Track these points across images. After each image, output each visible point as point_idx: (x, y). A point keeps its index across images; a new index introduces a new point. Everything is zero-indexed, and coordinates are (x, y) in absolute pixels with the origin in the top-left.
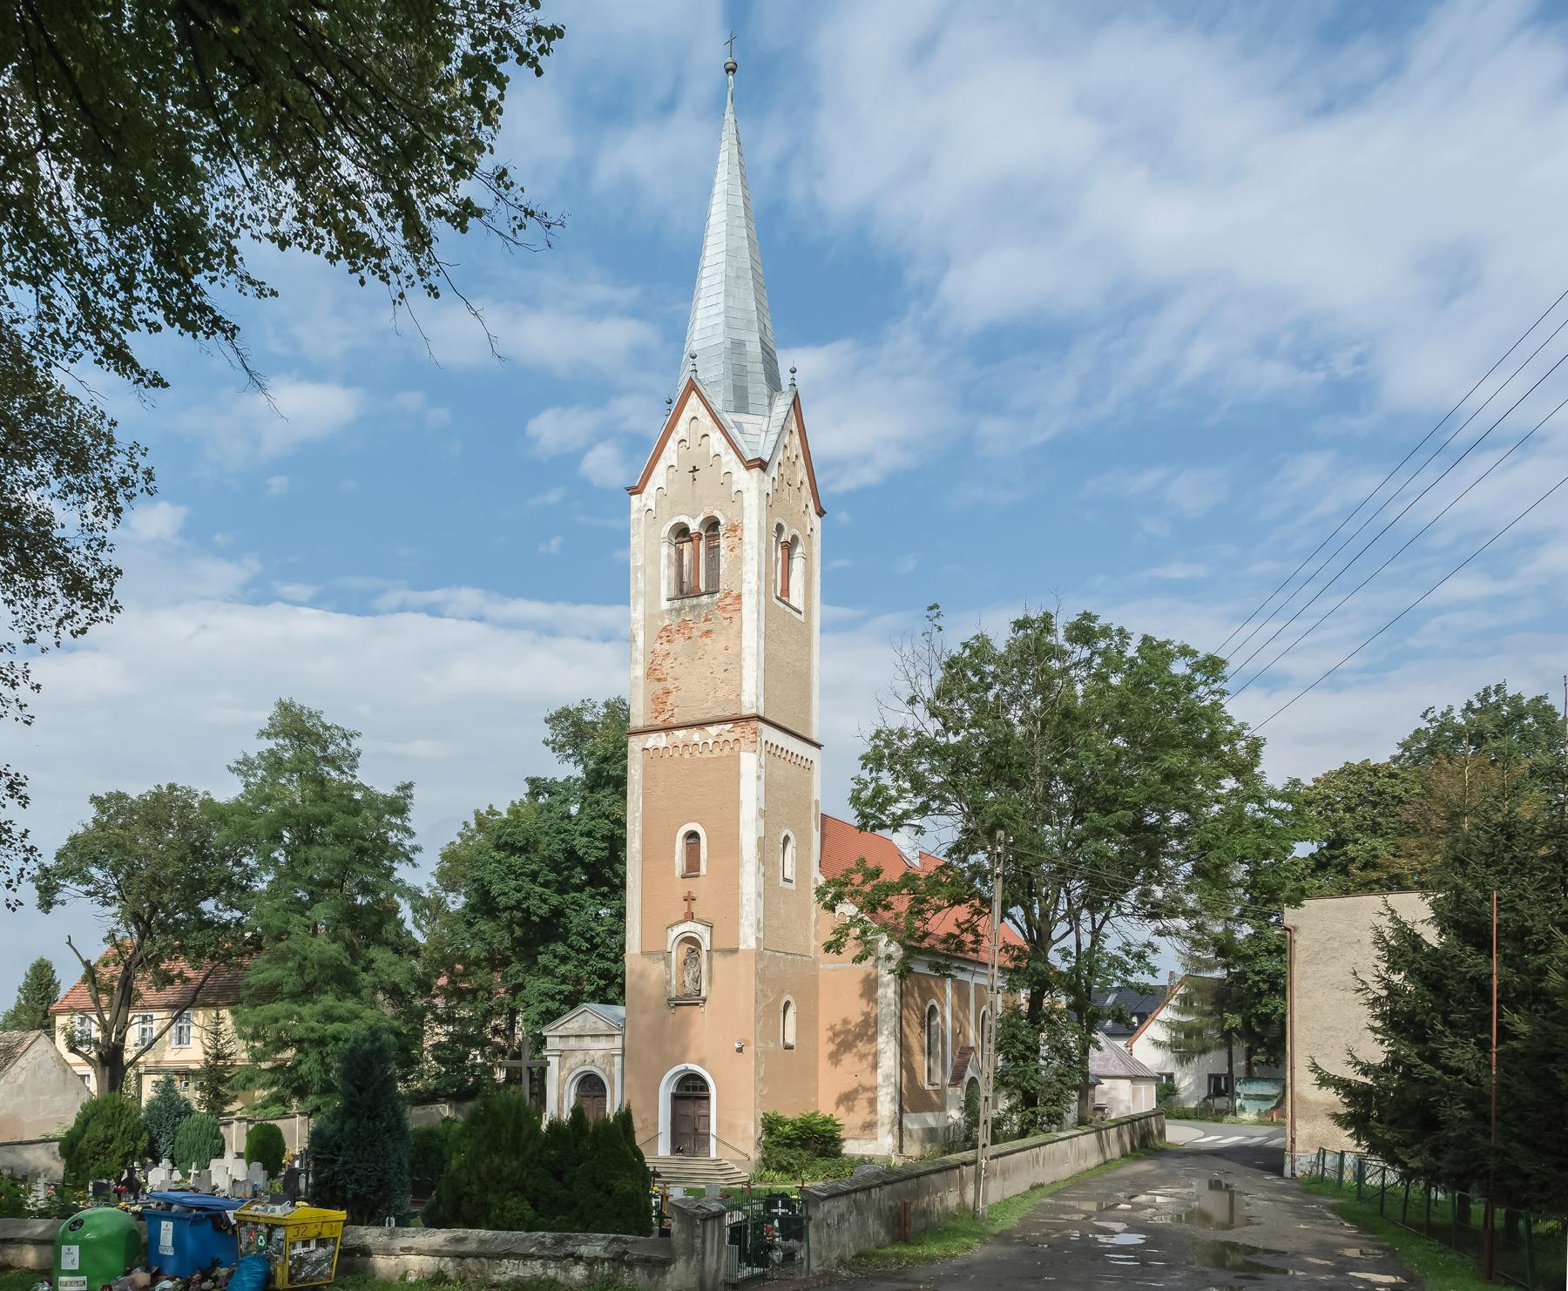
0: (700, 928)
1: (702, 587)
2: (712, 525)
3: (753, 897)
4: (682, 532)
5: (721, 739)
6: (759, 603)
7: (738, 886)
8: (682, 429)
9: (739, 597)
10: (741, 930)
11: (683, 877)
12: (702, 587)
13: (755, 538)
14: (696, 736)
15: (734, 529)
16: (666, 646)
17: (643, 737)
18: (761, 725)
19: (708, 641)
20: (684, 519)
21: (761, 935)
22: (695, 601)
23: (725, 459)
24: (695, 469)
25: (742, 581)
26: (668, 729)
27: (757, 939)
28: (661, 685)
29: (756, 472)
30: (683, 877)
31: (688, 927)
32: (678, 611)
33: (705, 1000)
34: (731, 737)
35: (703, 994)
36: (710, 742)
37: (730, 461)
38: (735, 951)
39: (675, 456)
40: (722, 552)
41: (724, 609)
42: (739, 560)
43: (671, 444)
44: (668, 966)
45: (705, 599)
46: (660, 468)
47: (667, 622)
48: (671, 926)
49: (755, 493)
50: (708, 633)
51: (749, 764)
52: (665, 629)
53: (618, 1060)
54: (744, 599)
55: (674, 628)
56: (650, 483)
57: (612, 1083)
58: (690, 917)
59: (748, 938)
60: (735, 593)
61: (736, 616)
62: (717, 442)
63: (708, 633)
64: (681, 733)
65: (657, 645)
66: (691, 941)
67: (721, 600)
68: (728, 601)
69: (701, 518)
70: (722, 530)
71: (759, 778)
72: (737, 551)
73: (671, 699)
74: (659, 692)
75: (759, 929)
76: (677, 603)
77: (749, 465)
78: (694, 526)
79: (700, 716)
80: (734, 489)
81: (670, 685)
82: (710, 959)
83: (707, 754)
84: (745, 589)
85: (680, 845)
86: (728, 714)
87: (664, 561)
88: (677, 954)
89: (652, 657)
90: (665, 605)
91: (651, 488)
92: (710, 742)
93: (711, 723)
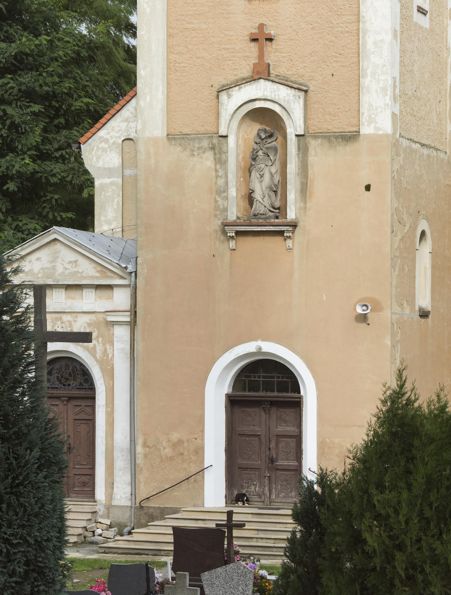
10: (365, 99)
31: (262, 92)
35: (291, 215)
38: (351, 137)
44: (221, 160)
57: (109, 374)
59: (378, 115)
66: (267, 120)
82: (303, 150)
88: (238, 139)
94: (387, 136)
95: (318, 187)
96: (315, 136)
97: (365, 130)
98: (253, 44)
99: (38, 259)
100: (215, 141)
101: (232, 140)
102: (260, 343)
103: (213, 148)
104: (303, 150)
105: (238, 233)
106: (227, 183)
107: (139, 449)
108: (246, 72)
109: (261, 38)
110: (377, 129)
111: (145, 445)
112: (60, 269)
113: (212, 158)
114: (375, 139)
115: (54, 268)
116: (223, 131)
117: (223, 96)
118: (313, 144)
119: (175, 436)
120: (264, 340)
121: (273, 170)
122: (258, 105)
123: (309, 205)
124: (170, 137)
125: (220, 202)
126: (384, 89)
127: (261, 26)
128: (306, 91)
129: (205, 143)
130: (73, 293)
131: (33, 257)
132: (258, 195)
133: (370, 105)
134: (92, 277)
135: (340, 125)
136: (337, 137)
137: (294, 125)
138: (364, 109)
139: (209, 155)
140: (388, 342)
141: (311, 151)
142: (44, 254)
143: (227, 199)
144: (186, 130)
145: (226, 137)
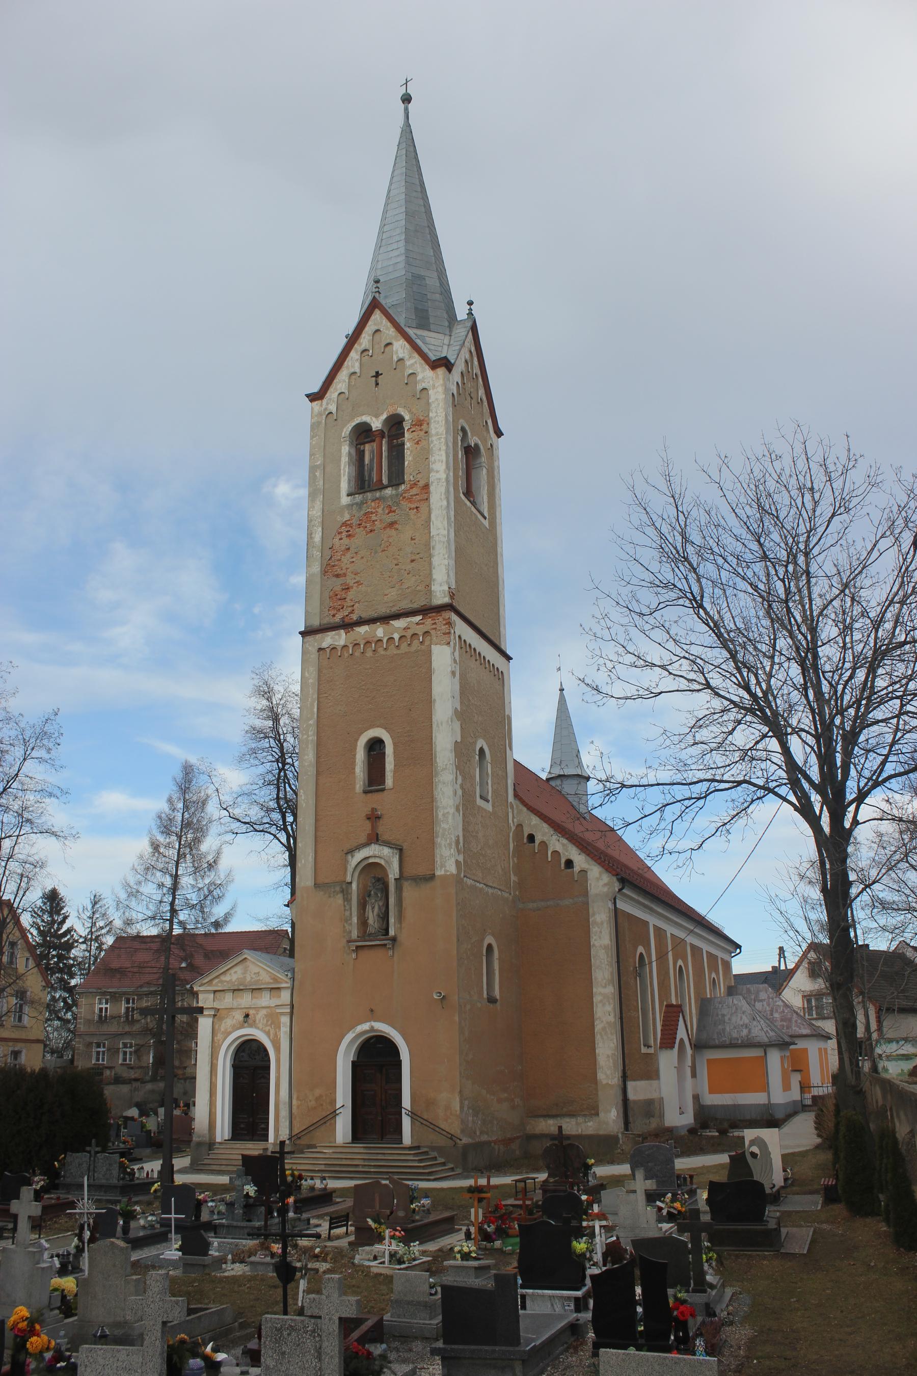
0: (386, 851)
1: (385, 481)
2: (395, 424)
3: (452, 810)
4: (363, 433)
5: (409, 634)
6: (447, 491)
7: (432, 799)
8: (365, 340)
9: (426, 487)
10: (437, 851)
11: (365, 792)
12: (385, 481)
13: (442, 430)
14: (380, 631)
15: (420, 423)
16: (346, 541)
17: (319, 636)
18: (454, 617)
19: (393, 532)
20: (366, 418)
21: (461, 858)
22: (378, 494)
23: (408, 363)
24: (377, 375)
25: (429, 471)
26: (347, 626)
27: (457, 862)
28: (340, 581)
29: (441, 371)
30: (365, 792)
31: (372, 851)
32: (360, 505)
33: (394, 939)
34: (420, 630)
35: (392, 932)
36: (396, 636)
37: (414, 363)
39: (357, 365)
40: (408, 445)
41: (410, 500)
42: (425, 456)
43: (354, 355)
45: (389, 491)
46: (343, 375)
47: (347, 517)
48: (351, 852)
49: (440, 389)
50: (392, 524)
51: (442, 658)
52: (344, 524)
53: (285, 1020)
54: (432, 488)
55: (355, 522)
56: (331, 389)
57: (277, 1049)
58: (374, 838)
59: (447, 862)
60: (421, 483)
61: (423, 507)
62: (400, 348)
63: (392, 524)
64: (363, 629)
65: (336, 540)
67: (405, 491)
68: (414, 491)
69: (384, 416)
70: (406, 426)
71: (453, 673)
72: (423, 443)
73: (351, 595)
74: (338, 588)
75: (459, 852)
76: (358, 498)
77: (434, 365)
78: (376, 424)
79: (383, 610)
80: (419, 387)
81: (350, 580)
83: (392, 651)
84: (433, 477)
85: (360, 755)
86: (415, 606)
87: (345, 459)
89: (328, 553)
90: (345, 500)
91: (332, 394)
92: (396, 636)
93: (397, 616)
94: (452, 875)
95: (409, 913)
96: (407, 879)
97: (439, 873)
98: (368, 822)
99: (236, 972)
100: (344, 887)
101: (354, 886)
102: (373, 1024)
103: (342, 891)
104: (399, 889)
105: (357, 947)
106: (351, 914)
107: (294, 1102)
108: (363, 839)
109: (374, 817)
110: (446, 871)
111: (298, 1099)
112: (248, 979)
113: (342, 898)
114: (444, 878)
115: (245, 977)
116: (349, 879)
117: (349, 857)
118: (406, 885)
119: (317, 1092)
120: (375, 1021)
121: (381, 904)
122: (371, 860)
123: (403, 925)
124: (316, 885)
125: (347, 927)
126: (450, 845)
127: (374, 810)
128: (401, 850)
129: (338, 889)
130: (256, 993)
131: (232, 971)
132: (371, 921)
133: (441, 855)
134: (269, 983)
135: (422, 870)
136: (421, 879)
137: (393, 872)
138: (438, 859)
139: (340, 896)
140: (457, 1018)
141: (405, 889)
142: (238, 969)
143: (351, 924)
144: (326, 881)
145: (351, 883)
